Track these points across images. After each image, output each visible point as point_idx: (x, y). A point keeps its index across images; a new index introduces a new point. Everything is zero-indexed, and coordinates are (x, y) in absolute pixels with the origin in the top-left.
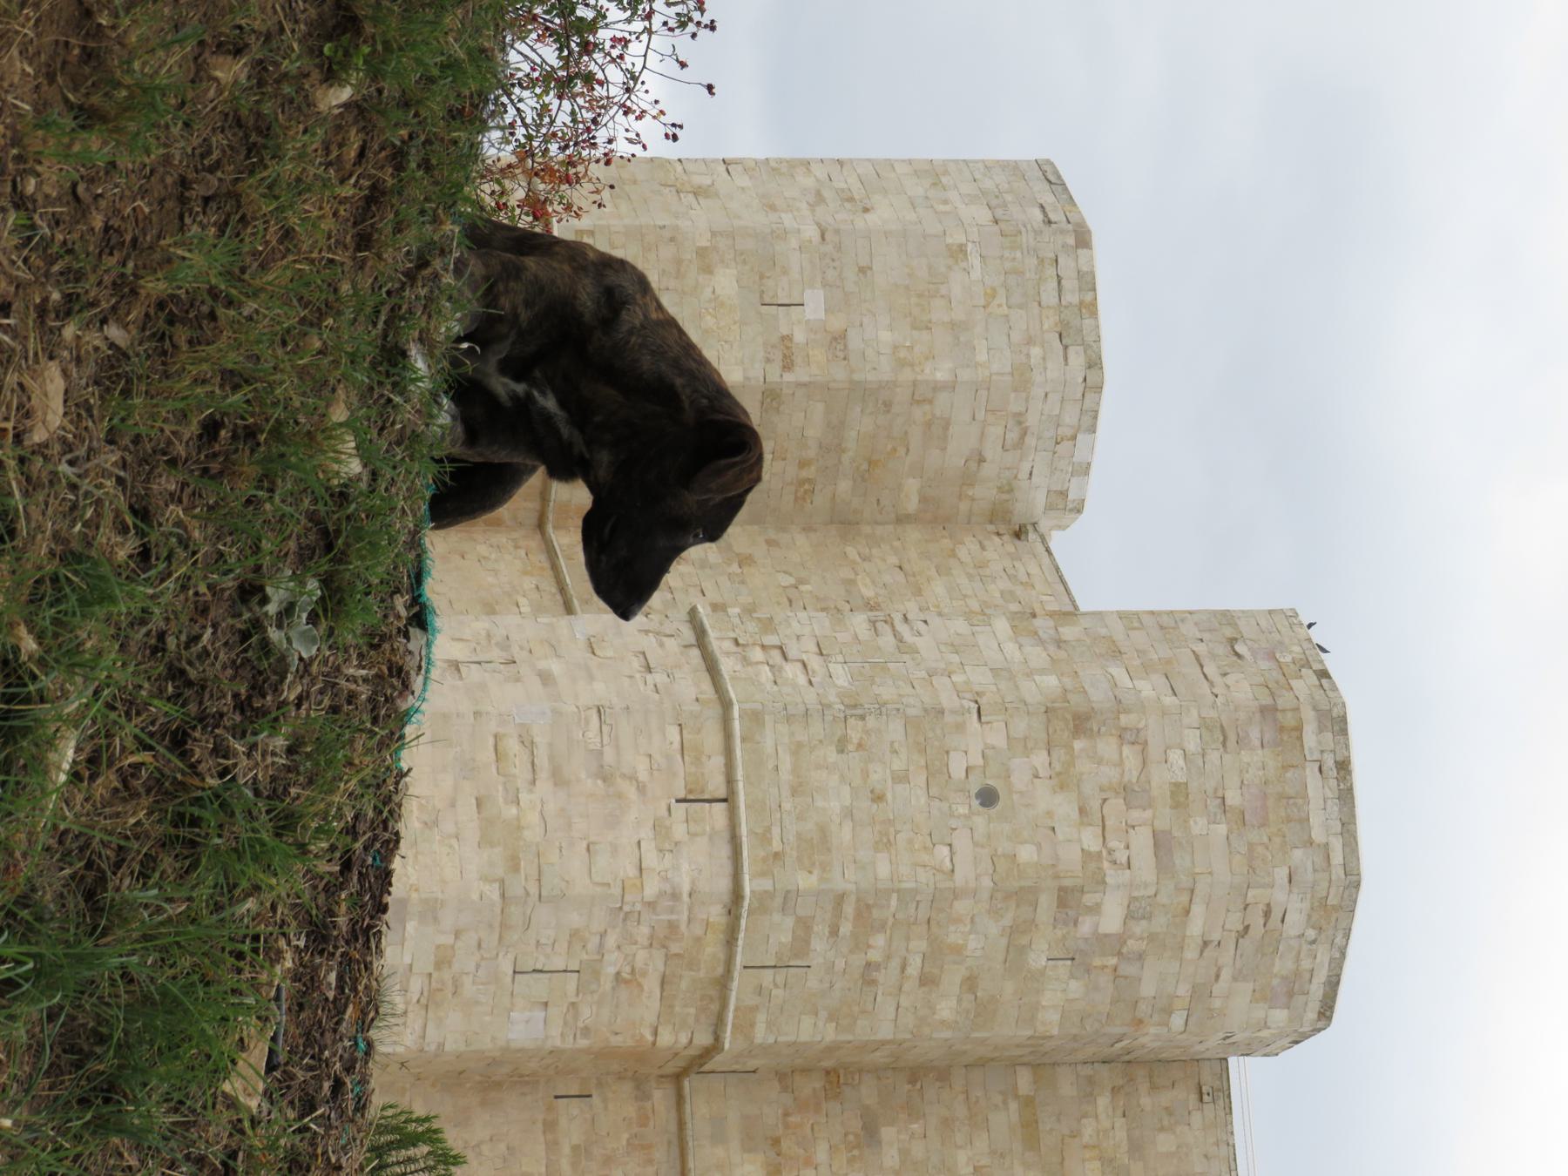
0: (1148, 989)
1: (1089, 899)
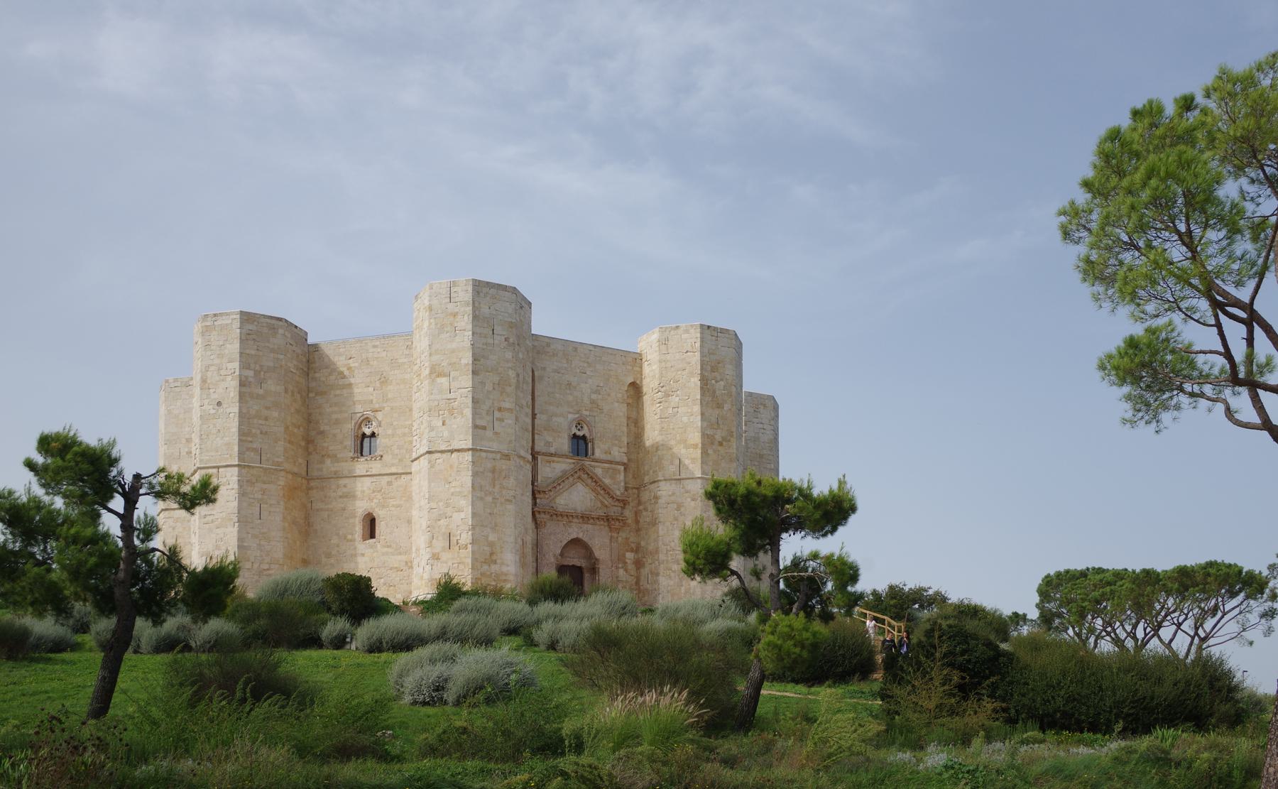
0: (271, 364)
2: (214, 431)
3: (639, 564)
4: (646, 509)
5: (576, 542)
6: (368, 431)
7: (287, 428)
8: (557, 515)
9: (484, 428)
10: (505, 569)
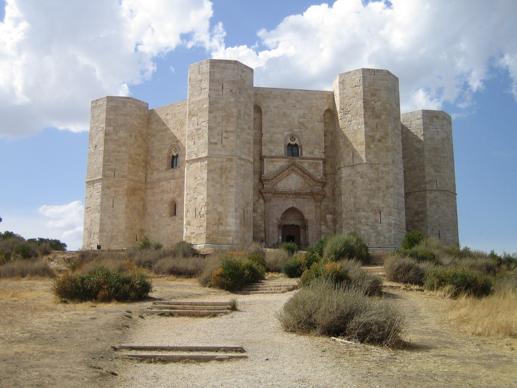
1: (107, 132)
2: (93, 162)
3: (335, 221)
4: (337, 186)
5: (292, 210)
6: (175, 154)
7: (130, 156)
8: (277, 194)
9: (216, 144)
10: (228, 228)
